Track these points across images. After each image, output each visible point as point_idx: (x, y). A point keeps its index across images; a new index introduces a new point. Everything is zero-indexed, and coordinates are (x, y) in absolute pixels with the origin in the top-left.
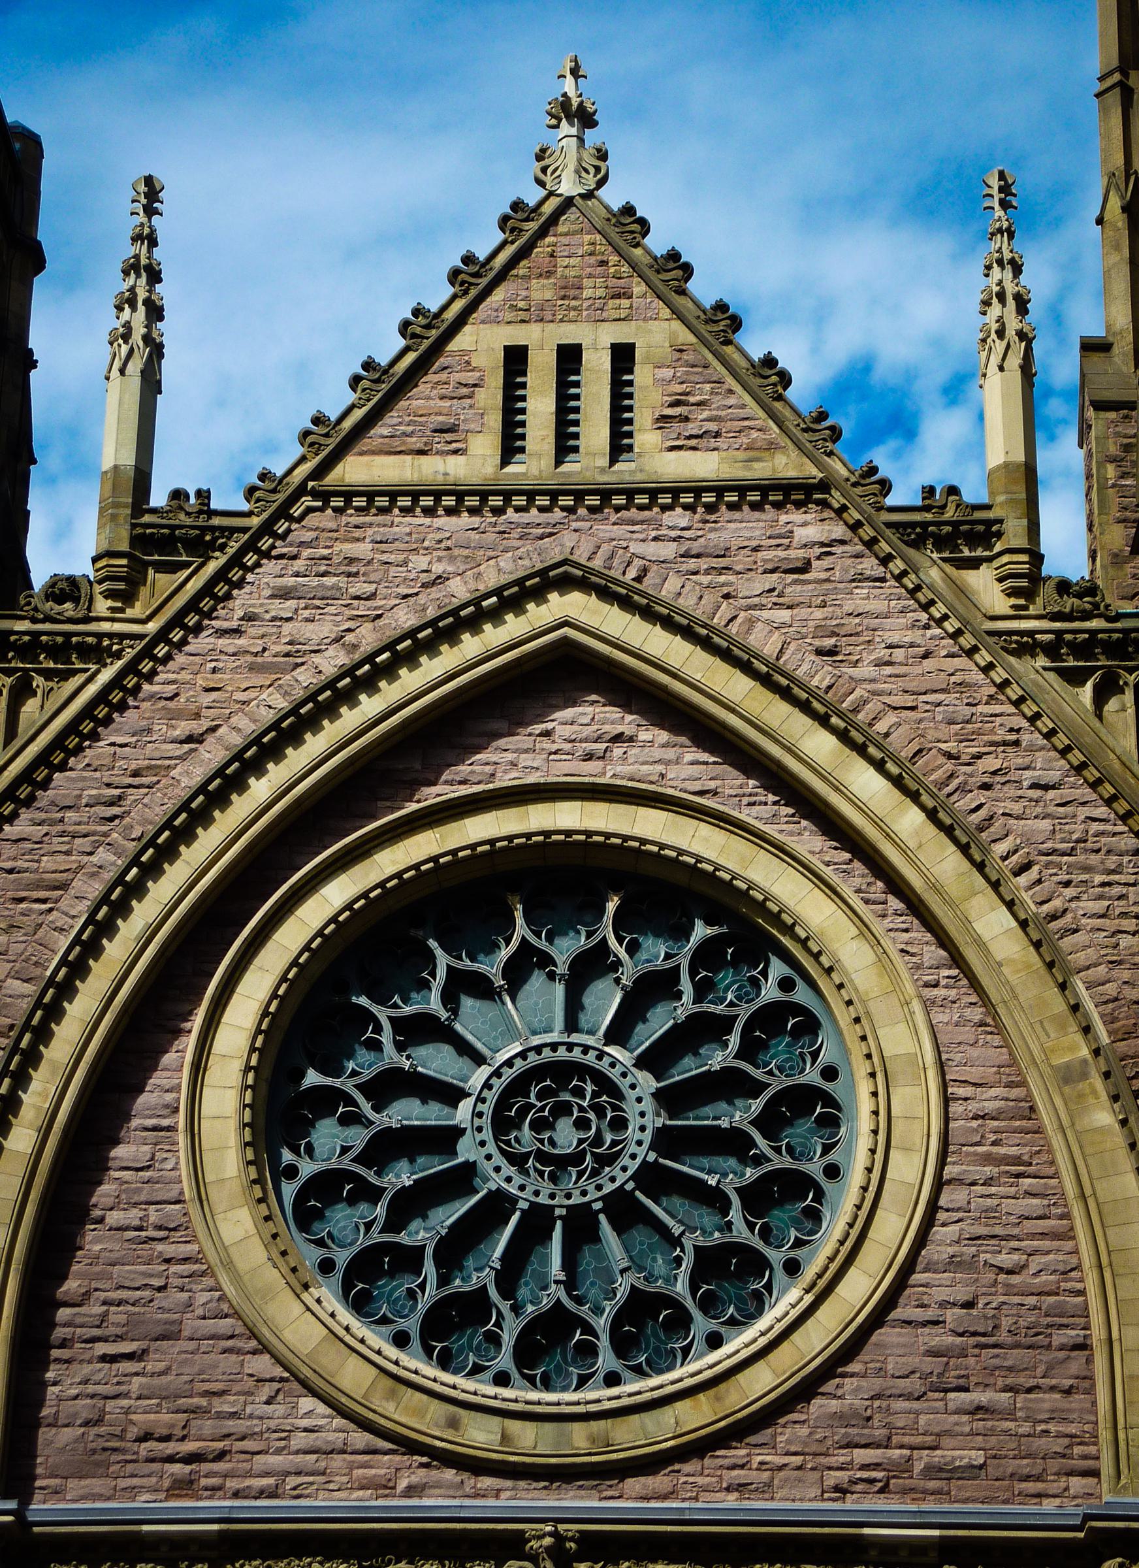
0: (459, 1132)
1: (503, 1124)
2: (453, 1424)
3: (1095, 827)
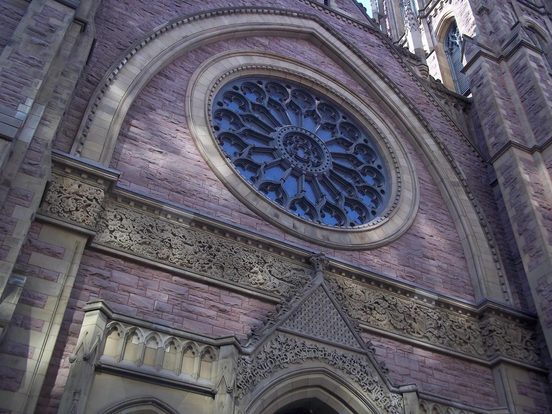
3: (450, 131)
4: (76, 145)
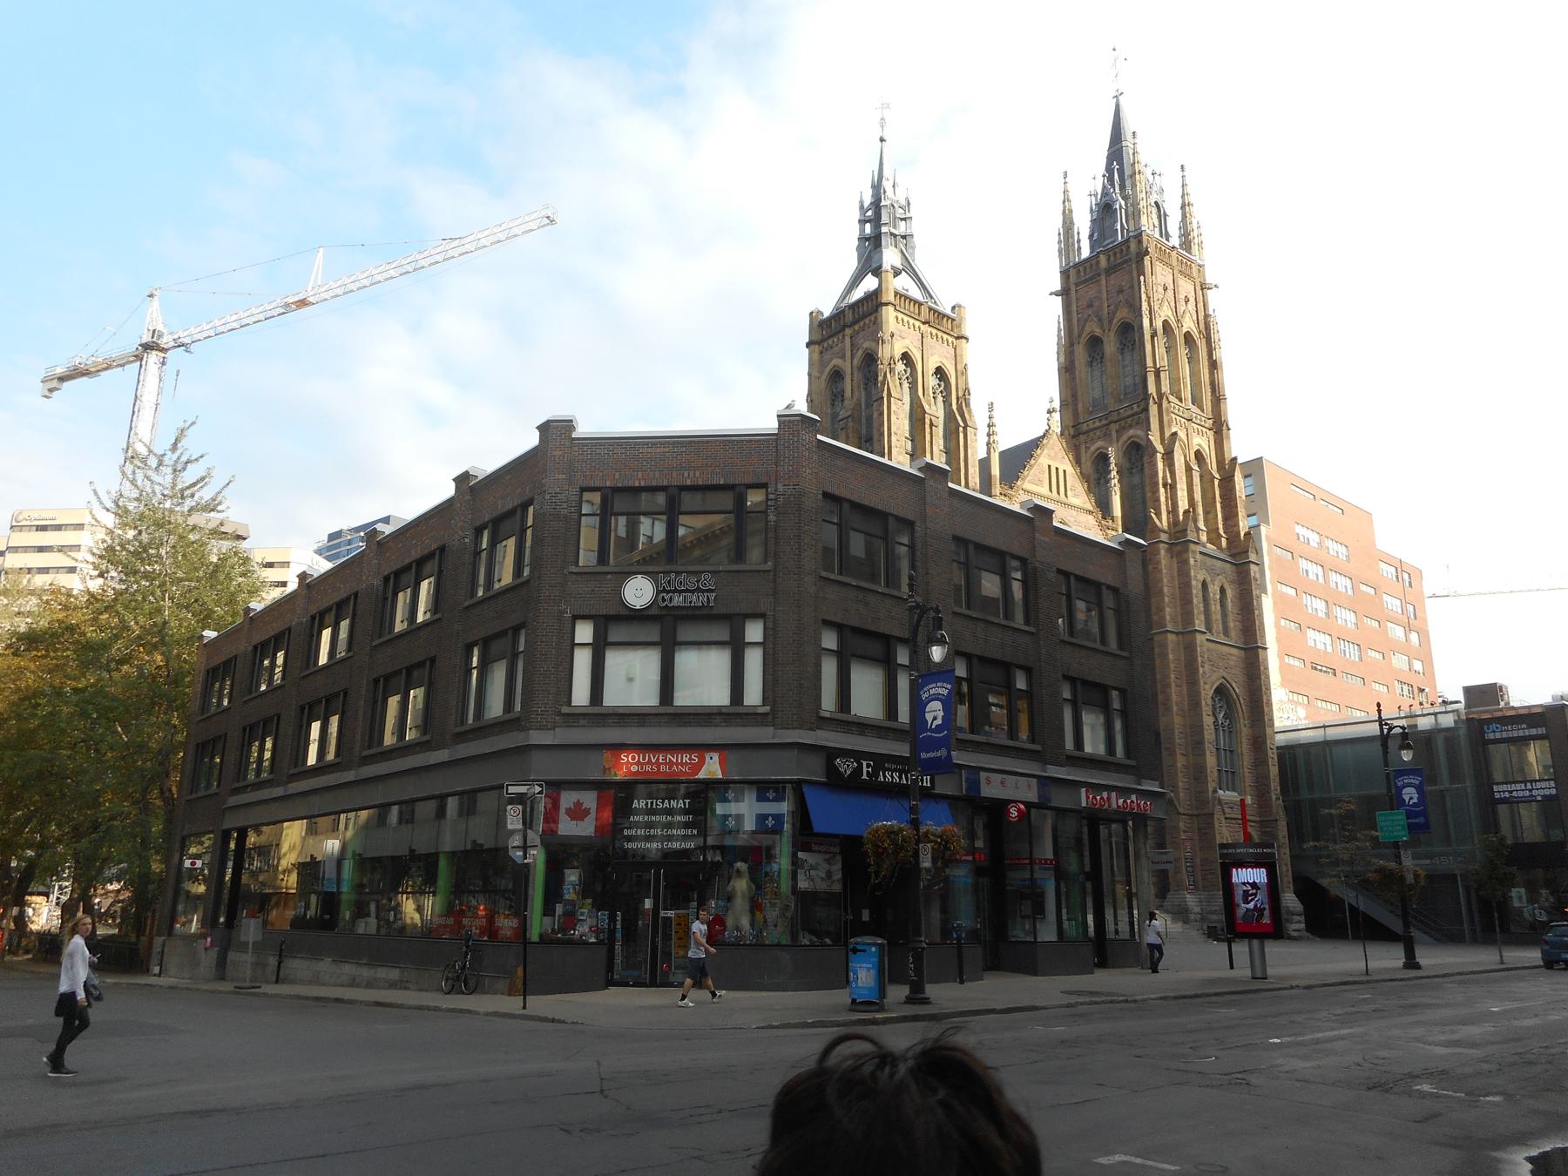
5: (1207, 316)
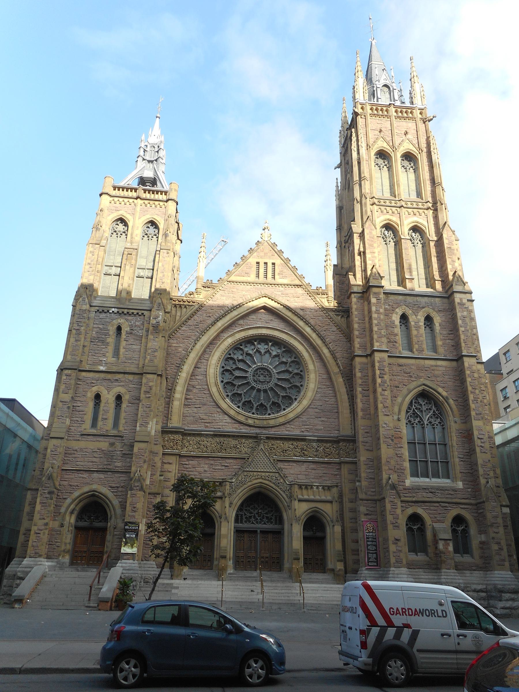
0: (247, 377)
1: (254, 376)
2: (247, 420)
4: (169, 420)
5: (428, 138)
